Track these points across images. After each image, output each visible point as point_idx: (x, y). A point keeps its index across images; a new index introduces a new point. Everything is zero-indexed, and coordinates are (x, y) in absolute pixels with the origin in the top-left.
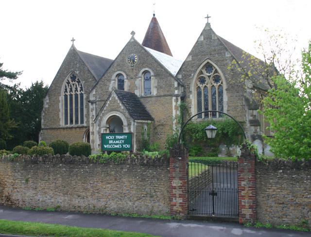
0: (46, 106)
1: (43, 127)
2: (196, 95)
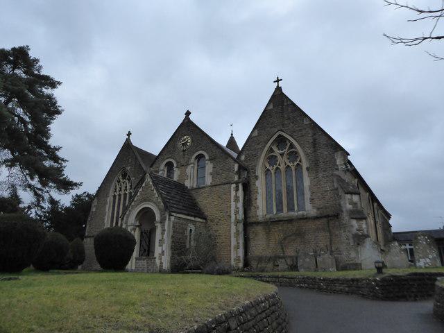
0: (94, 209)
1: (86, 234)
2: (264, 182)
